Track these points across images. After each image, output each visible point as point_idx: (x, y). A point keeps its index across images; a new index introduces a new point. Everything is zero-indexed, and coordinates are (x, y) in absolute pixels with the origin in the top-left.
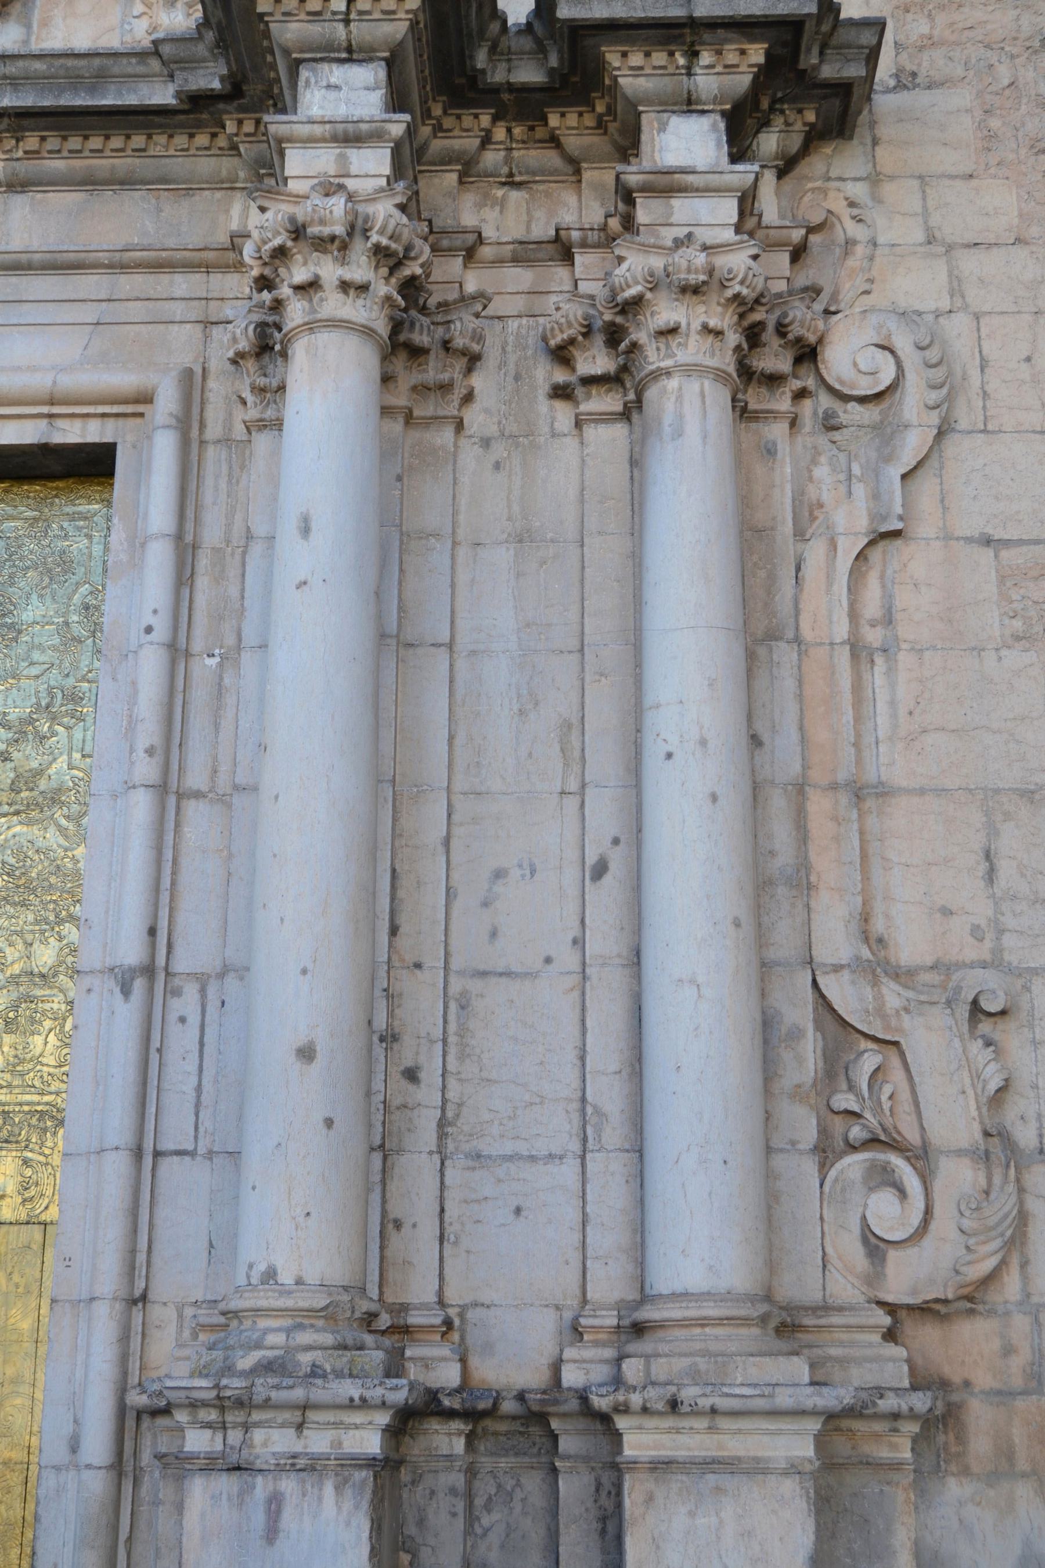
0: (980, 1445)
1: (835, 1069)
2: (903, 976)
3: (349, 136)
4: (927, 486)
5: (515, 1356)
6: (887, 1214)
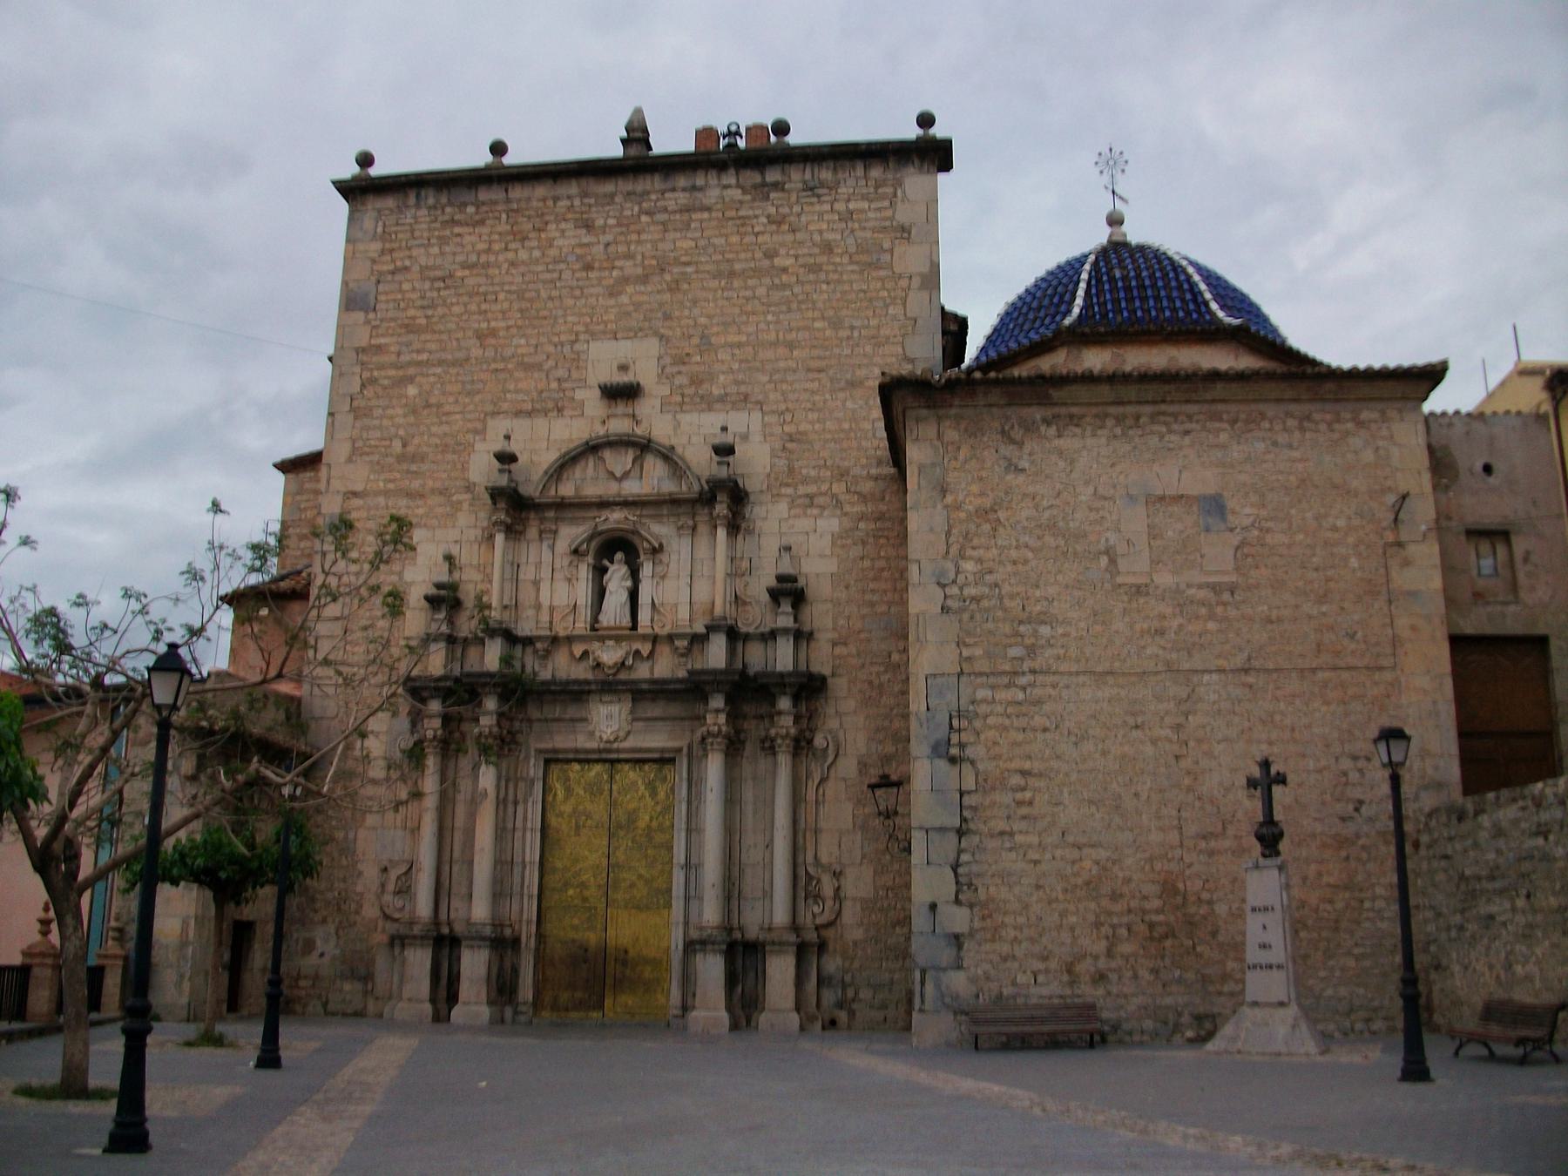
0: (831, 948)
1: (808, 884)
2: (822, 866)
3: (717, 711)
4: (832, 771)
5: (753, 933)
6: (816, 909)
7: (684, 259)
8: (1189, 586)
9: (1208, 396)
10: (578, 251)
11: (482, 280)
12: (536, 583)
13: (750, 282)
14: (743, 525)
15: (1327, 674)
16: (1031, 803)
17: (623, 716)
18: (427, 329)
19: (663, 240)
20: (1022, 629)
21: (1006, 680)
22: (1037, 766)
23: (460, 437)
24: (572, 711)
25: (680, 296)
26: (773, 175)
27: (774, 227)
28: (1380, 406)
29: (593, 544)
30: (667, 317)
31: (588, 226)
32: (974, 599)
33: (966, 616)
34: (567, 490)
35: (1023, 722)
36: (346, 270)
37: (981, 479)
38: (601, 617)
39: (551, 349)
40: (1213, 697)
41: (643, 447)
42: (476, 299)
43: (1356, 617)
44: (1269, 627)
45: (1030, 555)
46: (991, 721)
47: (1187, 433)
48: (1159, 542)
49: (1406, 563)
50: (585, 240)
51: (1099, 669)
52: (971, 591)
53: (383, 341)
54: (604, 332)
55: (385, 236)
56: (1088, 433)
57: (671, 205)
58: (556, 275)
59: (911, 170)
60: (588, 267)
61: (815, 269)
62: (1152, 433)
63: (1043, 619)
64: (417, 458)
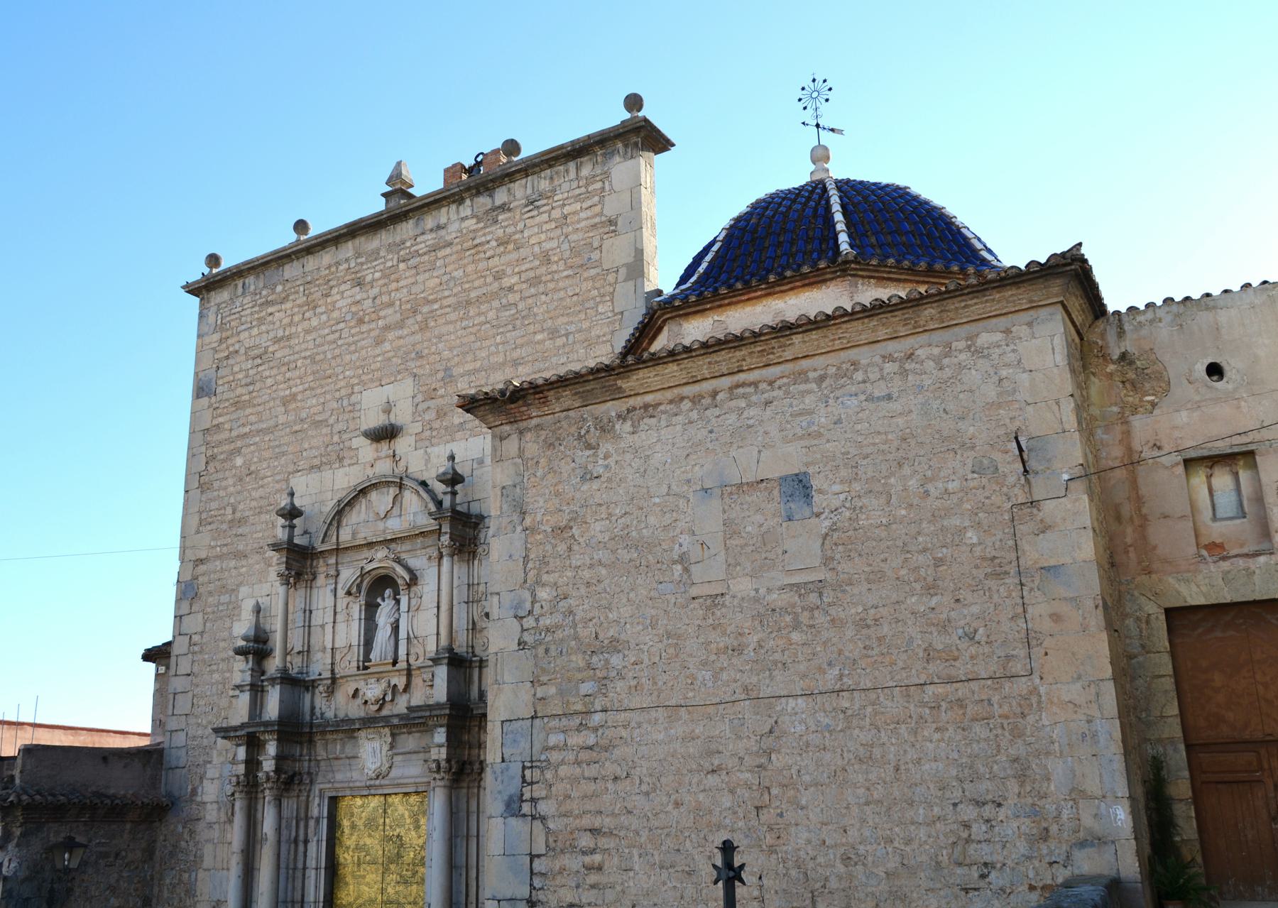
3: (440, 746)
7: (431, 297)
8: (769, 590)
9: (788, 355)
10: (354, 309)
11: (287, 351)
13: (484, 307)
14: (480, 550)
15: (940, 690)
16: (600, 868)
17: (384, 752)
18: (250, 403)
19: (415, 283)
20: (595, 659)
21: (577, 721)
22: (608, 822)
23: (272, 500)
24: (349, 750)
25: (428, 334)
26: (501, 196)
27: (502, 249)
28: (1002, 322)
30: (420, 356)
31: (360, 283)
32: (548, 630)
33: (541, 650)
34: (345, 536)
35: (591, 771)
36: (198, 361)
37: (557, 494)
38: (372, 656)
39: (335, 405)
40: (800, 729)
42: (284, 369)
43: (975, 609)
44: (864, 631)
45: (604, 572)
46: (563, 771)
47: (768, 403)
48: (736, 542)
49: (1045, 528)
50: (358, 298)
51: (673, 702)
52: (546, 621)
53: (221, 420)
54: (372, 380)
55: (220, 328)
56: (663, 423)
57: (422, 248)
58: (337, 335)
59: (617, 159)
60: (361, 321)
61: (535, 281)
62: (731, 410)
63: (615, 645)
64: (242, 521)
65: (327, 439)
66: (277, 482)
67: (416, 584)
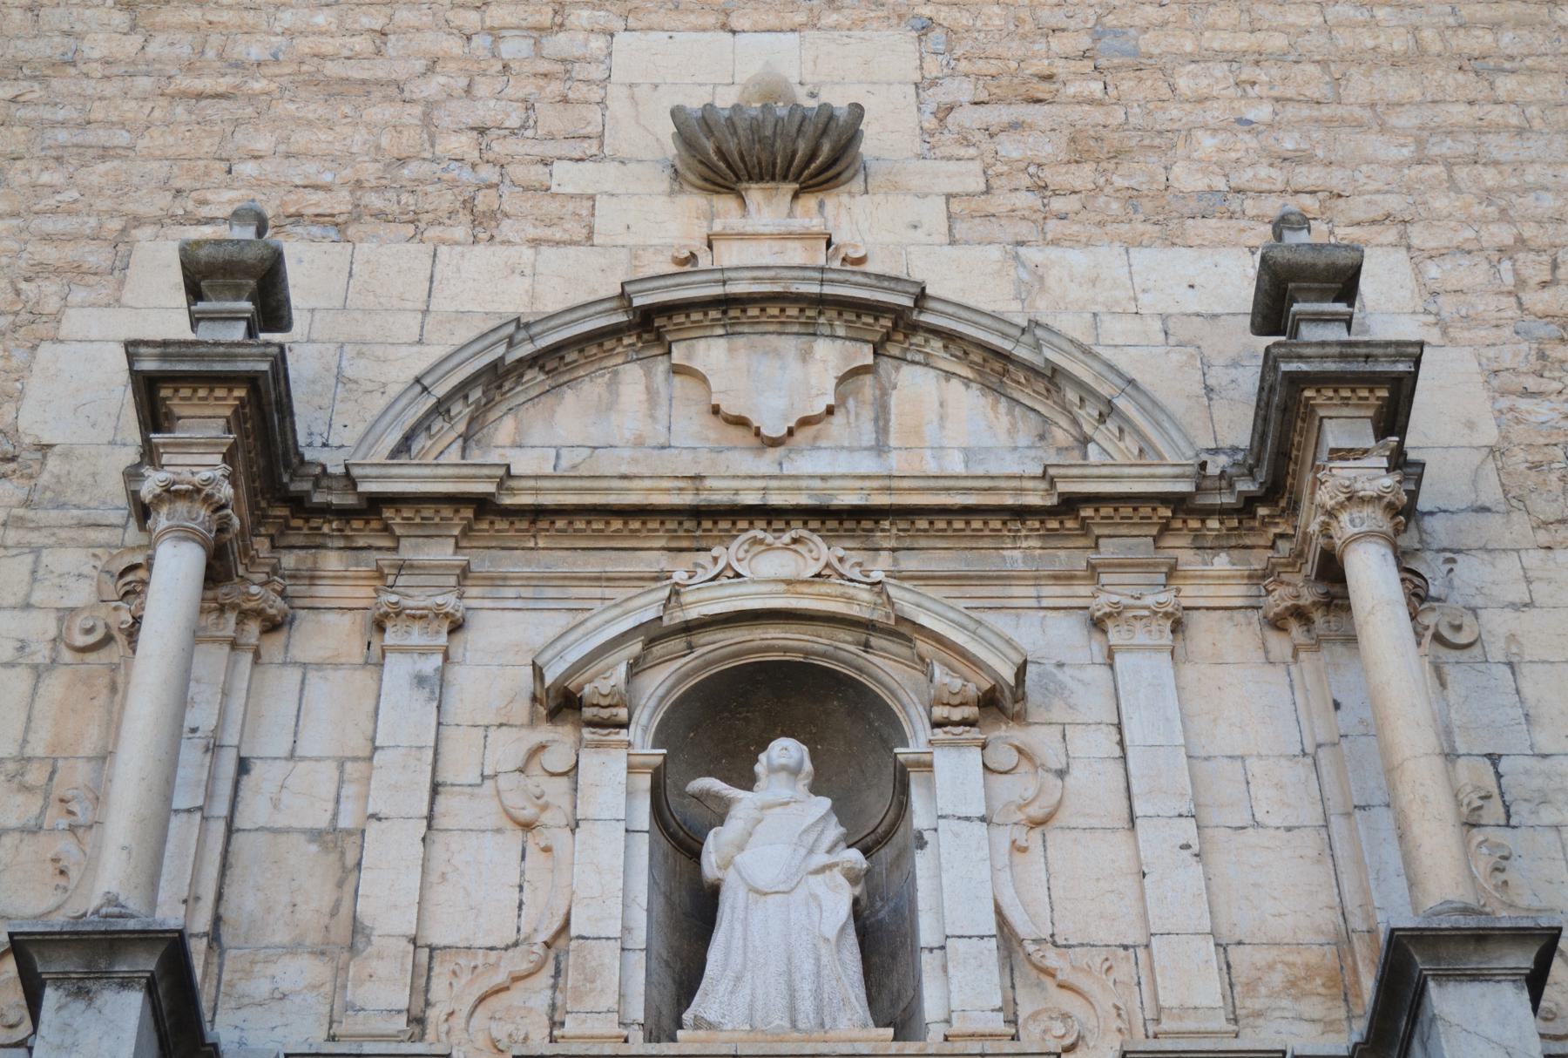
12: (341, 845)
29: (660, 684)
39: (455, 46)
41: (893, 322)
65: (411, 139)
66: (47, 238)
67: (1019, 718)
